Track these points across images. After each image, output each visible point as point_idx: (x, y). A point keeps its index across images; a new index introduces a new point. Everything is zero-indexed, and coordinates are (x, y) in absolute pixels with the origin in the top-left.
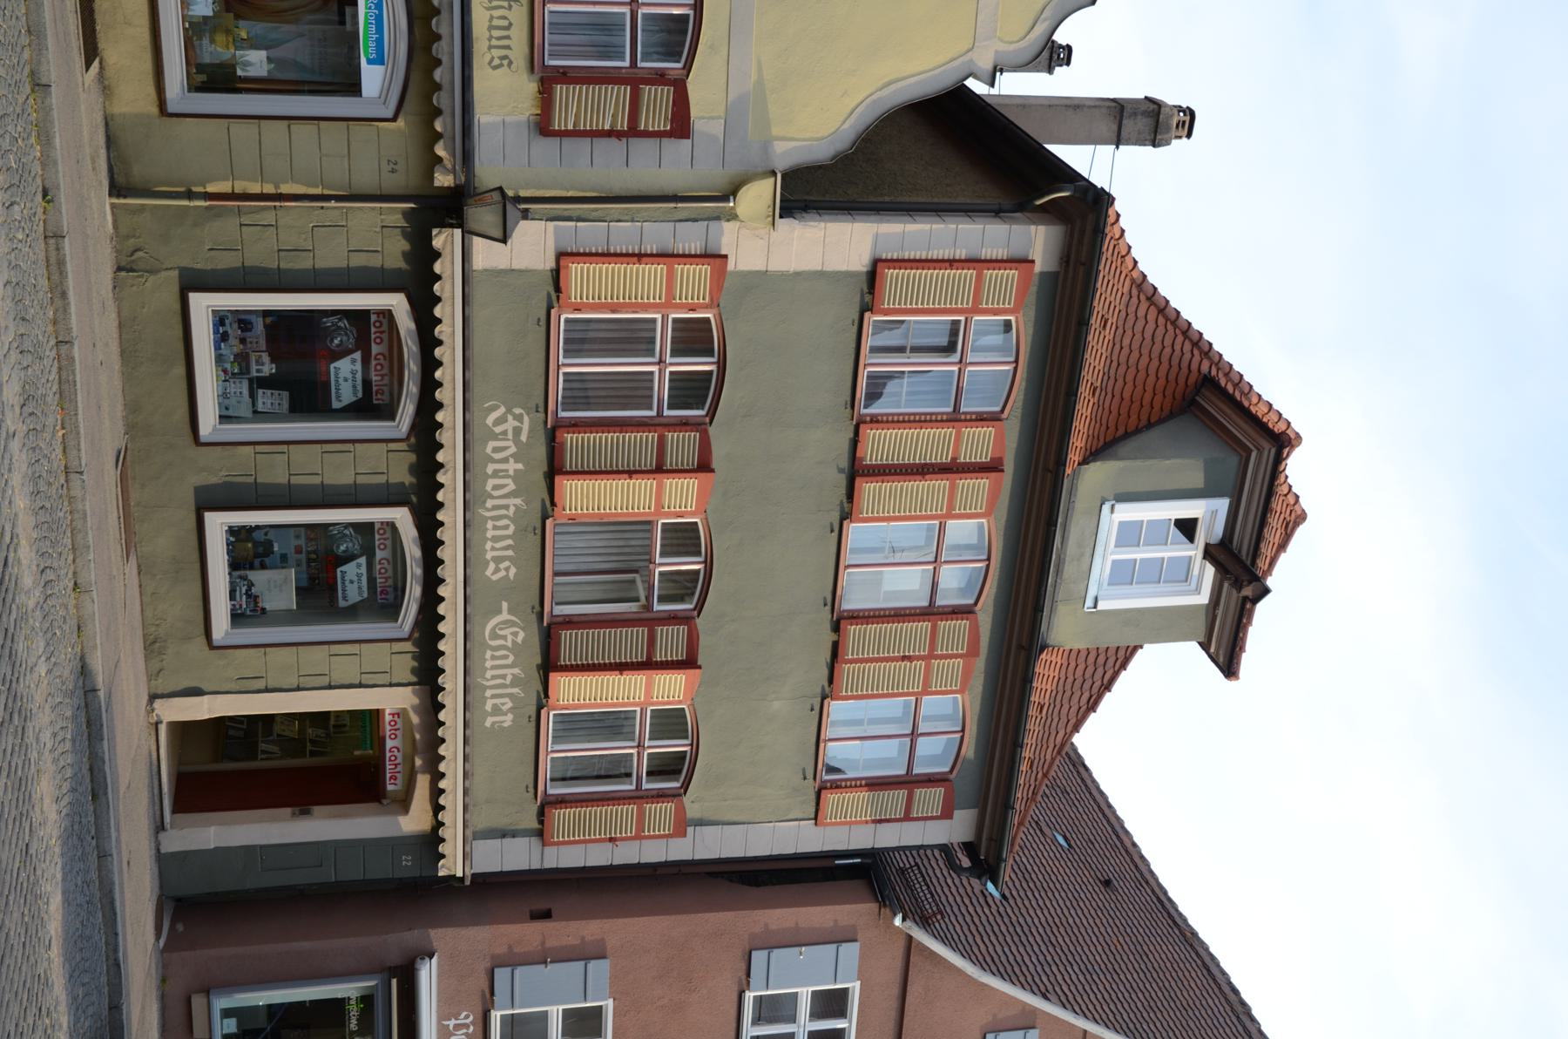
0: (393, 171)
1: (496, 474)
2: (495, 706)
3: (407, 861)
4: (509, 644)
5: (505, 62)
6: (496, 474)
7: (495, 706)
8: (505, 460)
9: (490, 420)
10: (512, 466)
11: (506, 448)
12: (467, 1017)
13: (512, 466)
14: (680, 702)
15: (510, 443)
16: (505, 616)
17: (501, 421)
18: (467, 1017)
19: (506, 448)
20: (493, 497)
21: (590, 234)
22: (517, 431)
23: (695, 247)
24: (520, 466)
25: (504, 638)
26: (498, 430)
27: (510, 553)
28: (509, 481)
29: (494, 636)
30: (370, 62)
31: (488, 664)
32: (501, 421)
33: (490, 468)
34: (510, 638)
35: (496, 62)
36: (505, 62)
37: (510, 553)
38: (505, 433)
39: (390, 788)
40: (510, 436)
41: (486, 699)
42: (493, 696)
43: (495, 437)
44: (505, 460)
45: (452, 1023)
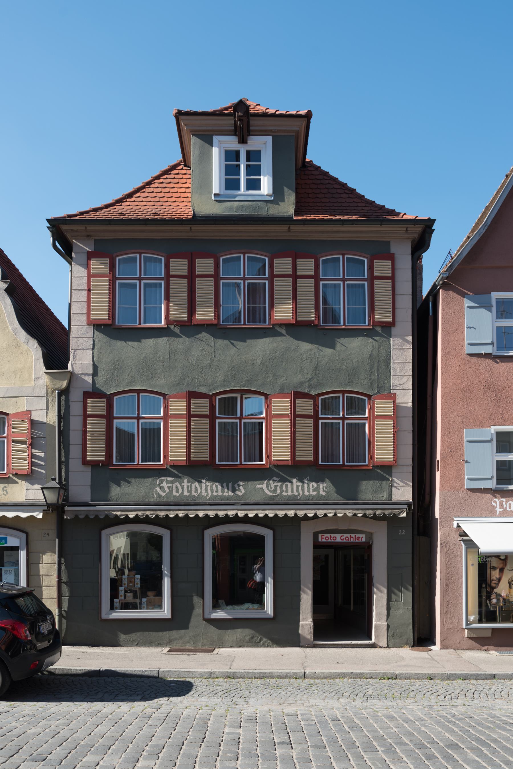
0: (48, 534)
1: (189, 491)
2: (314, 490)
3: (402, 532)
4: (279, 484)
5: (5, 489)
6: (189, 491)
7: (314, 490)
8: (183, 487)
9: (163, 494)
10: (186, 484)
11: (177, 487)
12: (495, 502)
13: (186, 484)
14: (268, 457)
15: (174, 485)
16: (264, 486)
17: (162, 489)
18: (495, 502)
19: (177, 487)
20: (201, 492)
21: (75, 451)
22: (168, 482)
23: (80, 405)
24: (186, 480)
25: (276, 487)
26: (167, 490)
27: (230, 484)
28: (193, 485)
29: (275, 491)
30: (6, 543)
31: (290, 493)
32: (162, 489)
33: (186, 493)
34: (276, 484)
35: (5, 492)
36: (5, 489)
37: (230, 484)
38: (169, 487)
39: (364, 540)
40: (170, 485)
41: (310, 495)
42: (309, 491)
43: (171, 492)
44: (183, 487)
45: (498, 510)
